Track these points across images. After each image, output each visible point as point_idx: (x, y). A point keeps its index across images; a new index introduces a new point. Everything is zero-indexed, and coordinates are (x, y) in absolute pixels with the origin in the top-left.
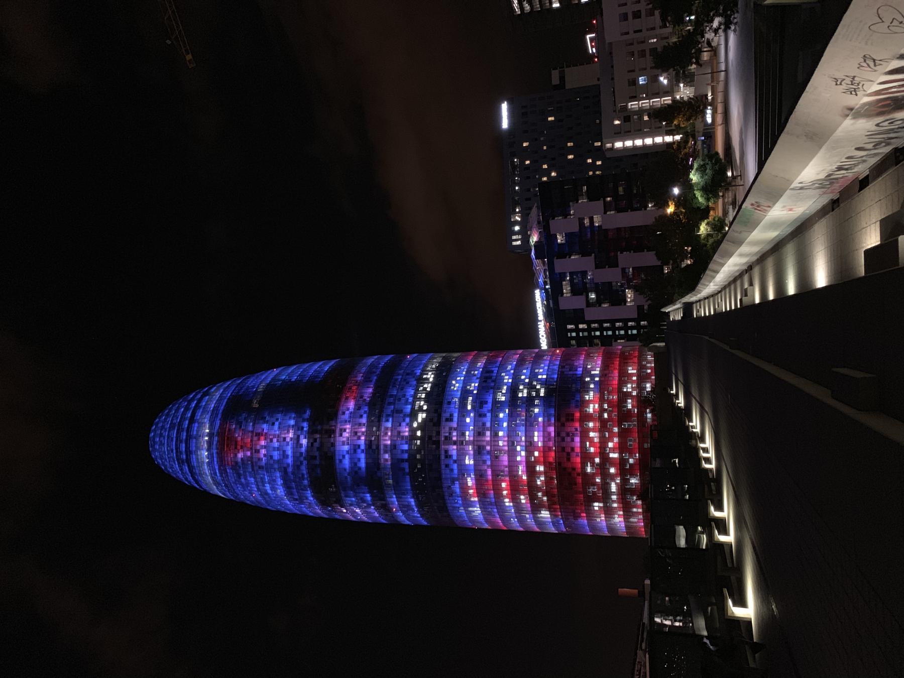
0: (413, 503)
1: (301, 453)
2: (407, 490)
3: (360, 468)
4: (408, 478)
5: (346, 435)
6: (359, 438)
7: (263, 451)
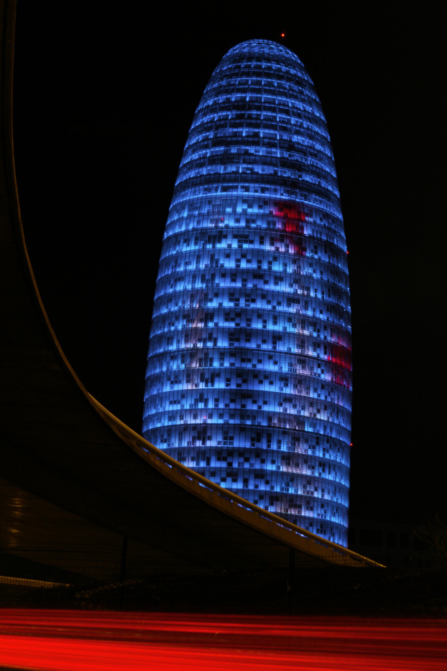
0: (209, 444)
1: (279, 304)
2: (232, 438)
3: (261, 382)
4: (248, 445)
5: (300, 371)
6: (295, 387)
7: (282, 249)
